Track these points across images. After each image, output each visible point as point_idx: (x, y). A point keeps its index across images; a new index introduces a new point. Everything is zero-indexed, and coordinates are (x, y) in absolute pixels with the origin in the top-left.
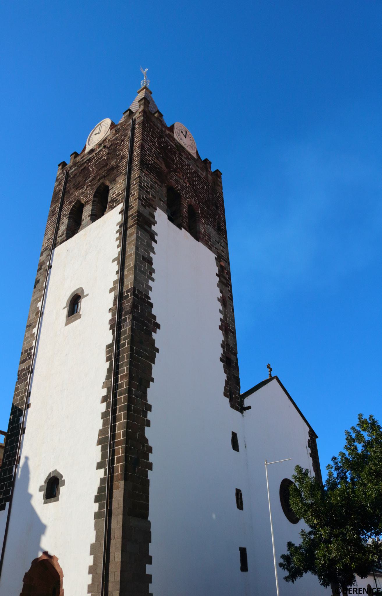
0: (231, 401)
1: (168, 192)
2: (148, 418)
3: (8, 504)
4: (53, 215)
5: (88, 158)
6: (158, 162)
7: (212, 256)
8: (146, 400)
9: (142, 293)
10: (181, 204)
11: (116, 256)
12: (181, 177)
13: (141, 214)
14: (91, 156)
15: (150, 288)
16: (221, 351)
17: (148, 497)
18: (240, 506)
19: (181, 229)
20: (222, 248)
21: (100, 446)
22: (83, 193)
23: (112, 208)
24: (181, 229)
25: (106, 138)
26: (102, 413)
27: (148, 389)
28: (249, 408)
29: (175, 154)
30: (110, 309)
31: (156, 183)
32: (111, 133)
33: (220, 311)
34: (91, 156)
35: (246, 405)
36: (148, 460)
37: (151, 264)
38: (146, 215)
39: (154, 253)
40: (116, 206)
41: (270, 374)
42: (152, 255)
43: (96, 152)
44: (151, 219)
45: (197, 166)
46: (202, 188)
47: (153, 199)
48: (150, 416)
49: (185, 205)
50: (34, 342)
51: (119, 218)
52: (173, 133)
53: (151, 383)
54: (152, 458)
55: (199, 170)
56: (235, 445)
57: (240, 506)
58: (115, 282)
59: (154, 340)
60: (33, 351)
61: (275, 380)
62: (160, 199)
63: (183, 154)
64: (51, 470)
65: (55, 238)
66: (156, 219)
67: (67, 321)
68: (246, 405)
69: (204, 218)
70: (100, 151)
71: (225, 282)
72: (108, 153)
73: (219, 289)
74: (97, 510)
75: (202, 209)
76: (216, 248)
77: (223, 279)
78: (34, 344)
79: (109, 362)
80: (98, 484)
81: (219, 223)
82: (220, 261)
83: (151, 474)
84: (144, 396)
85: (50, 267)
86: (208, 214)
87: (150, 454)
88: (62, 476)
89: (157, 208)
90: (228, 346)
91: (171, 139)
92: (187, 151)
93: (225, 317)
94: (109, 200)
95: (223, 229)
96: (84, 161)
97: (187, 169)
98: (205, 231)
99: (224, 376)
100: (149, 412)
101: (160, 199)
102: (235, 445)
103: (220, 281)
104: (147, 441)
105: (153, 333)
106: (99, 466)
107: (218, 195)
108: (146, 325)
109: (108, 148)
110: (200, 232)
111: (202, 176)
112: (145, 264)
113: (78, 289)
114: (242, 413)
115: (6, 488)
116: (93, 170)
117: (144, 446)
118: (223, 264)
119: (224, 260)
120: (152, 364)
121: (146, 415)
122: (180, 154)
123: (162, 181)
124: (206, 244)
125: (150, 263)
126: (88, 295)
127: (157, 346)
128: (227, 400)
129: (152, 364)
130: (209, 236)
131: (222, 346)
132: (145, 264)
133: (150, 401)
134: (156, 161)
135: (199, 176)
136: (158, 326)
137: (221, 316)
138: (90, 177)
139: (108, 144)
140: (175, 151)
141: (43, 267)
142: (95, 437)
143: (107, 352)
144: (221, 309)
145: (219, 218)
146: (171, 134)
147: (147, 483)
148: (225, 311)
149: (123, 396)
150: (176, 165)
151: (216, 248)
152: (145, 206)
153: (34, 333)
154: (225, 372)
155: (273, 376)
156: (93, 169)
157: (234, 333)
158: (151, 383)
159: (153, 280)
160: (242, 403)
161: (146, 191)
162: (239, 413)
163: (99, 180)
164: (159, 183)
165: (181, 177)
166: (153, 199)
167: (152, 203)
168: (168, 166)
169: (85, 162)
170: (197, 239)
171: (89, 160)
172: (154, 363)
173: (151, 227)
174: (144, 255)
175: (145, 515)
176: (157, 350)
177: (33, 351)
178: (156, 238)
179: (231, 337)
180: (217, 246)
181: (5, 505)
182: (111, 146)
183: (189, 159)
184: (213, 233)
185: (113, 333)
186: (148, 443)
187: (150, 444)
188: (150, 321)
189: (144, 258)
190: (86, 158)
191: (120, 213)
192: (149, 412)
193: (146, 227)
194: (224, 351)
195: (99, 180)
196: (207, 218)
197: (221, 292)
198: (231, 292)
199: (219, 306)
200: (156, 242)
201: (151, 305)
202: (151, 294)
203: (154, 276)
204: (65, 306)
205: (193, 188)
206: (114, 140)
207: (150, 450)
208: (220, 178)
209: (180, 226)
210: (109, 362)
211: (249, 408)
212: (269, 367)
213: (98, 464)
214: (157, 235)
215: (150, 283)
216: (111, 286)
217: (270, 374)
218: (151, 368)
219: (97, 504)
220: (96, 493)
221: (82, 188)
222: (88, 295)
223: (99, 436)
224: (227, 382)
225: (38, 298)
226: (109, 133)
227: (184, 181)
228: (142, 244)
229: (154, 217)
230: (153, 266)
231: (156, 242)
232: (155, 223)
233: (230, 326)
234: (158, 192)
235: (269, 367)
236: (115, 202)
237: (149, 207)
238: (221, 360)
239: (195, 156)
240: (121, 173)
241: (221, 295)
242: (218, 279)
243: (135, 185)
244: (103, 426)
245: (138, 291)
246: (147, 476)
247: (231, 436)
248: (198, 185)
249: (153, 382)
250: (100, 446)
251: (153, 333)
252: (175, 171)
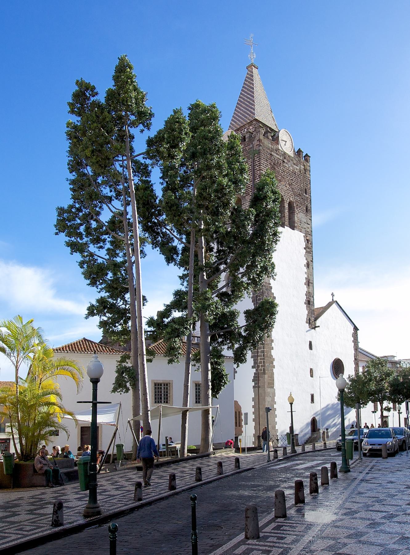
28: (319, 326)
35: (317, 325)
54: (275, 363)
56: (311, 347)
71: (309, 250)
83: (274, 370)
90: (309, 293)
93: (308, 276)
102: (311, 347)
131: (306, 295)
155: (334, 300)
157: (313, 283)
180: (306, 226)
197: (306, 259)
207: (274, 359)
211: (319, 326)
224: (308, 315)
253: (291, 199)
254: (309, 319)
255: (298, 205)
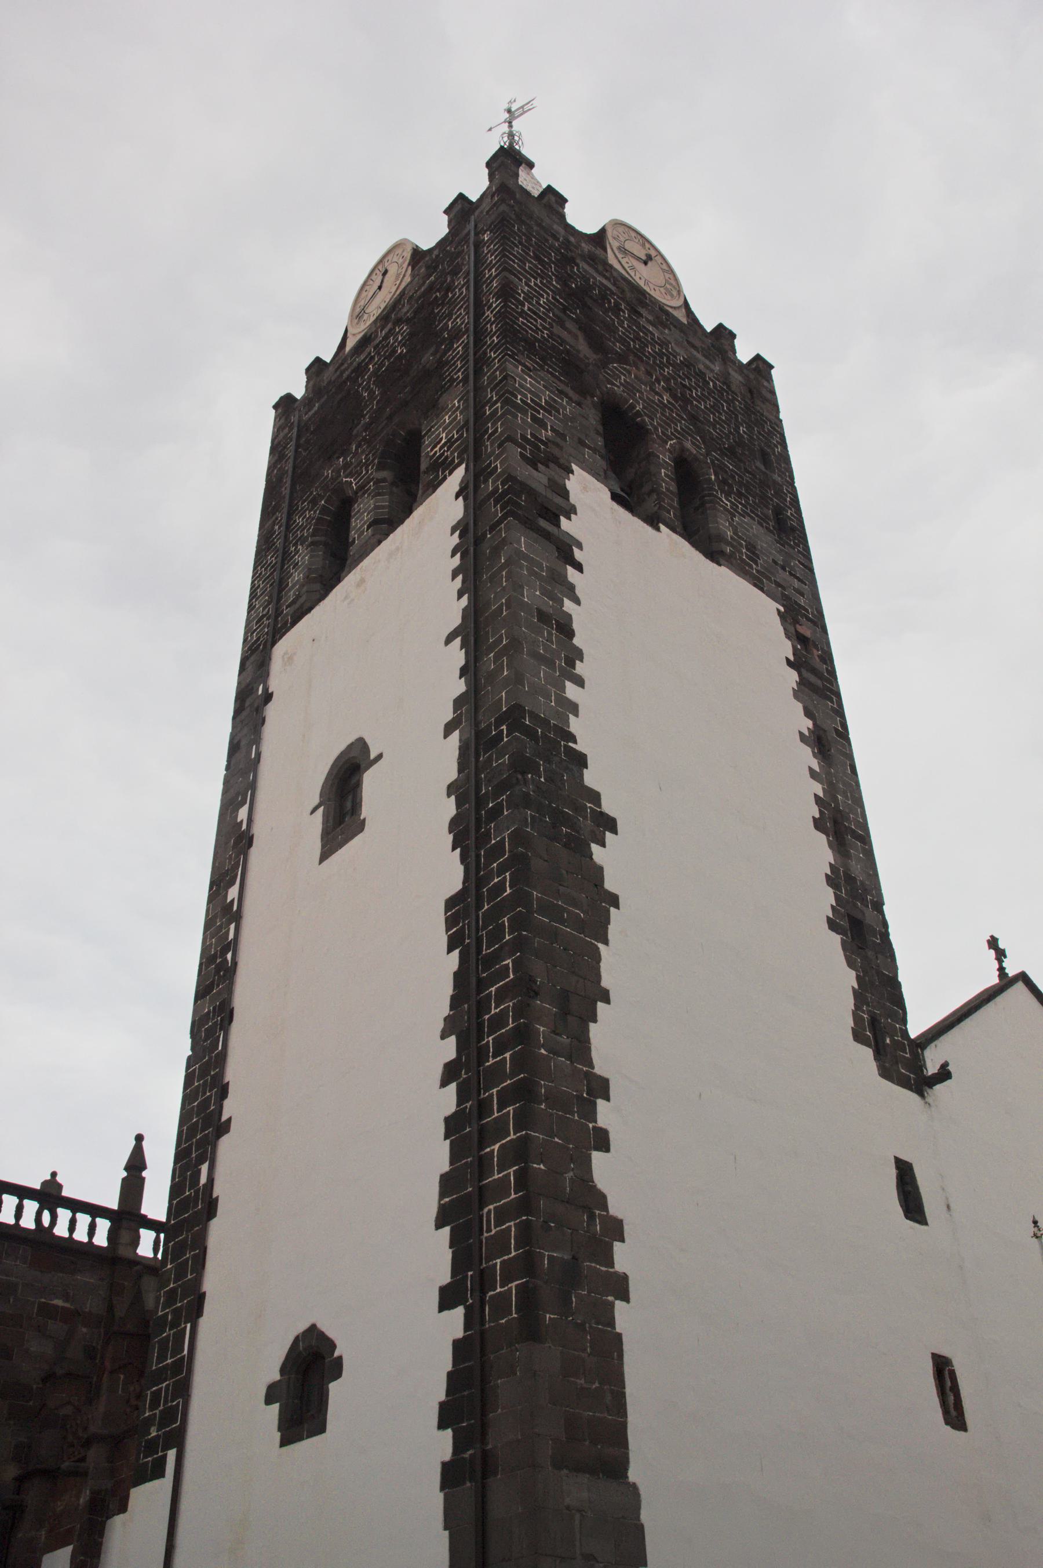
0: (879, 1053)
1: (605, 422)
2: (602, 1121)
3: (172, 1454)
4: (269, 549)
5: (355, 364)
6: (564, 334)
7: (768, 608)
8: (591, 1065)
9: (545, 722)
10: (650, 456)
11: (457, 621)
12: (643, 377)
13: (522, 484)
14: (362, 357)
15: (574, 708)
16: (828, 897)
17: (623, 1395)
18: (955, 1415)
19: (658, 529)
20: (796, 584)
21: (446, 1230)
22: (346, 466)
23: (434, 486)
24: (658, 529)
25: (403, 294)
26: (447, 1120)
27: (592, 1026)
29: (617, 310)
30: (449, 787)
31: (561, 393)
32: (413, 276)
33: (813, 774)
34: (362, 357)
36: (613, 1267)
37: (570, 634)
38: (541, 490)
39: (577, 601)
40: (445, 479)
41: (1001, 970)
42: (568, 605)
43: (377, 341)
44: (558, 500)
45: (688, 342)
46: (715, 408)
47: (558, 440)
48: (606, 1114)
49: (665, 458)
50: (232, 926)
51: (457, 510)
52: (605, 250)
53: (600, 1006)
55: (699, 356)
56: (912, 1205)
57: (955, 1415)
58: (458, 702)
59: (601, 869)
60: (229, 956)
61: (1020, 986)
62: (581, 442)
63: (643, 311)
64: (302, 1327)
65: (278, 613)
66: (573, 499)
67: (323, 847)
68: (932, 1068)
69: (728, 495)
70: (386, 337)
72: (411, 335)
73: (799, 707)
74: (447, 1454)
75: (719, 468)
76: (778, 585)
77: (813, 679)
78: (231, 936)
79: (456, 953)
80: (445, 1362)
81: (778, 512)
82: (795, 622)
83: (625, 1318)
84: (581, 1049)
85: (268, 697)
86: (740, 484)
87: (617, 1246)
88: (333, 1346)
89: (574, 467)
90: (850, 879)
91: (600, 268)
92: (654, 302)
93: (831, 789)
94: (423, 466)
95: (793, 529)
96: (345, 375)
97: (661, 354)
98: (735, 533)
99: (849, 978)
100: (601, 1103)
101: (581, 442)
102: (912, 1205)
103: (802, 682)
104: (601, 1200)
105: (595, 848)
106: (448, 1299)
107: (767, 427)
108: (567, 821)
109: (408, 321)
110: (721, 538)
111: (709, 375)
112: (550, 634)
113: (350, 746)
114: (921, 1095)
115: (166, 1402)
116: (371, 393)
117: (592, 1217)
118: (806, 630)
119: (808, 619)
120: (601, 946)
121: (591, 1113)
122: (634, 311)
123: (584, 391)
124: (742, 570)
125: (566, 629)
126: (380, 756)
127: (610, 884)
128: (867, 1053)
129: (601, 946)
130: (751, 548)
131: (832, 881)
132: (550, 634)
133: (601, 1067)
134: (557, 330)
135: (701, 375)
136: (610, 824)
137: (818, 789)
138: (364, 416)
139: (406, 310)
140: (617, 304)
141: (247, 704)
142: (430, 1200)
143: (450, 923)
144: (815, 765)
145: (779, 493)
146: (599, 252)
147: (611, 1347)
148: (828, 774)
149: (507, 1055)
150: (623, 341)
151: (778, 585)
152: (533, 463)
153: (233, 901)
154: (851, 964)
155: (1011, 972)
156: (369, 391)
158: (600, 1006)
159: (580, 682)
160: (917, 1064)
161: (534, 419)
162: (913, 1097)
163: (390, 418)
164: (571, 393)
165: (643, 377)
166: (558, 440)
167: (556, 451)
168: (596, 343)
169: (349, 378)
170: (714, 555)
171: (360, 370)
172: (606, 942)
173: (558, 525)
174: (544, 608)
175: (615, 1467)
176: (614, 900)
177: (229, 956)
178: (578, 554)
179: (856, 851)
180: (782, 576)
181: (165, 1457)
182: (416, 312)
183: (665, 326)
184: (766, 541)
185: (463, 859)
186: (605, 1207)
187: (615, 1209)
188: (580, 809)
189: (543, 617)
190: (351, 363)
191: (457, 497)
192: (601, 1103)
193: (543, 523)
194: (837, 898)
195: (390, 418)
196: (740, 494)
197: (808, 713)
198: (840, 712)
199: (807, 758)
200: (579, 567)
201: (581, 760)
202: (575, 725)
203: (580, 668)
204: (316, 800)
205: (684, 408)
206: (424, 295)
208: (769, 379)
209: (653, 521)
210: (456, 953)
212: (993, 943)
213: (443, 1291)
214: (580, 546)
215: (571, 691)
216: (449, 715)
217: (1001, 970)
218: (597, 957)
219: (449, 1432)
220: (440, 1394)
221: (344, 453)
222: (380, 756)
223: (442, 1195)
225: (238, 794)
226: (408, 279)
227: (652, 390)
228: (532, 573)
229: (565, 494)
230: (576, 641)
231: (579, 567)
232: (570, 511)
233: (848, 819)
234: (573, 419)
235: (993, 943)
236: (443, 467)
237: (547, 466)
238: (832, 925)
239: (681, 316)
240: (452, 380)
241: (810, 723)
242: (793, 676)
243: (496, 402)
244: (451, 1163)
245: (534, 716)
246: (612, 1323)
247: (893, 1172)
248: (701, 398)
249: (607, 1001)
250: (446, 1230)
251: (595, 848)
252: (622, 359)
253: (688, 445)
254: (874, 1022)
255: (724, 482)
